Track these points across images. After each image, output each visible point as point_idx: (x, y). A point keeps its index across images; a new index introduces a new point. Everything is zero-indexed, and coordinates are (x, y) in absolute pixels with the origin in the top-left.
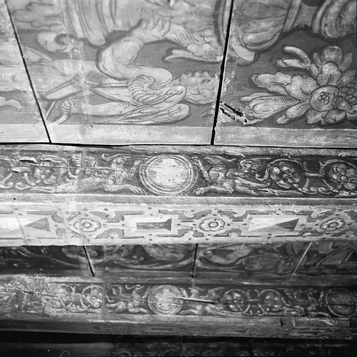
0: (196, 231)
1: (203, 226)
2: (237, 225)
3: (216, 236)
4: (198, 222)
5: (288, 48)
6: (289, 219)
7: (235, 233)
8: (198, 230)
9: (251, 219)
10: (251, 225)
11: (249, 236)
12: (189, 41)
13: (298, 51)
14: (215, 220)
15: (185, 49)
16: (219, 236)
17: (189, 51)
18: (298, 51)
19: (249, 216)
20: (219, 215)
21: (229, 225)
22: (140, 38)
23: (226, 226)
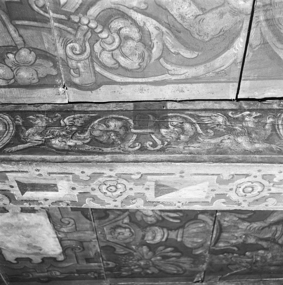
0: (270, 182)
1: (259, 188)
2: (222, 189)
3: (247, 175)
4: (265, 193)
5: (178, 221)
6: (166, 197)
7: (224, 178)
8: (268, 183)
9: (207, 197)
10: (206, 190)
11: (207, 174)
12: (237, 222)
13: (171, 220)
14: (245, 195)
15: (240, 218)
16: (244, 175)
17: (238, 217)
18: (171, 220)
19: (209, 200)
20: (241, 201)
21: (231, 189)
22: (265, 223)
23: (235, 188)
